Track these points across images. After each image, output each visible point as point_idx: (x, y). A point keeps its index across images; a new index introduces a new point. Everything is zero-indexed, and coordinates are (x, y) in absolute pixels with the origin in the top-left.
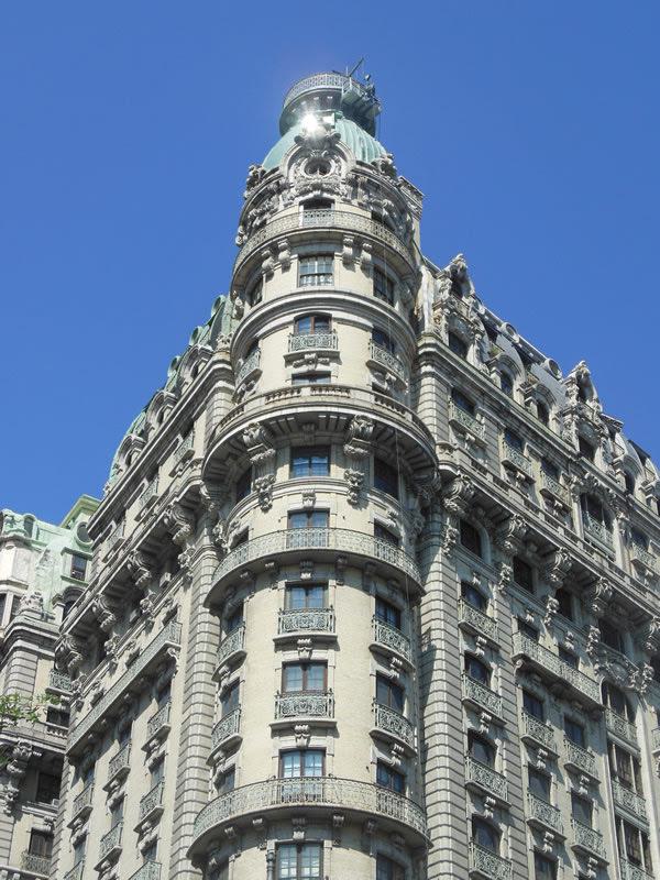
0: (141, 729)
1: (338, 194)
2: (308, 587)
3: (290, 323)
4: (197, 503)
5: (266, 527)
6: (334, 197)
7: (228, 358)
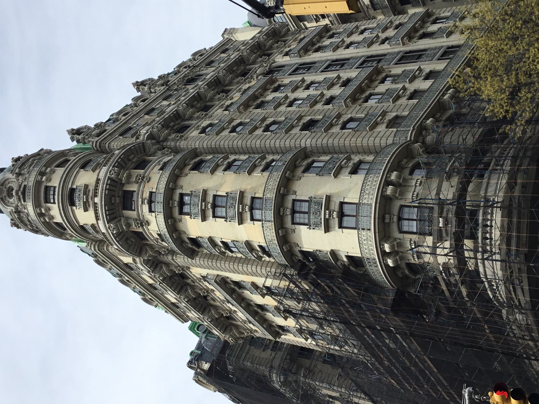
0: (257, 299)
1: (22, 183)
2: (182, 204)
3: (71, 208)
4: (153, 262)
5: (155, 225)
6: (23, 184)
7: (94, 243)
